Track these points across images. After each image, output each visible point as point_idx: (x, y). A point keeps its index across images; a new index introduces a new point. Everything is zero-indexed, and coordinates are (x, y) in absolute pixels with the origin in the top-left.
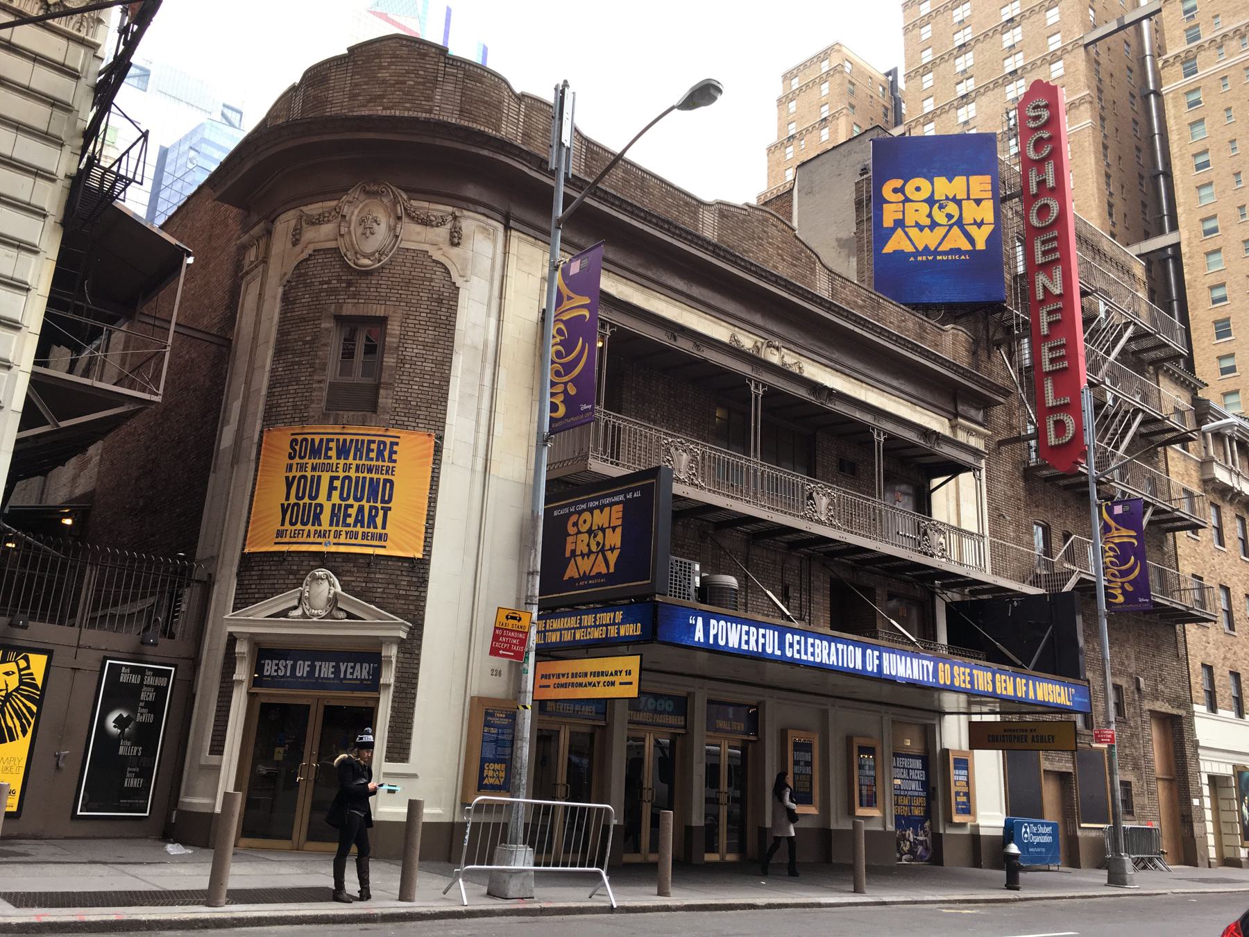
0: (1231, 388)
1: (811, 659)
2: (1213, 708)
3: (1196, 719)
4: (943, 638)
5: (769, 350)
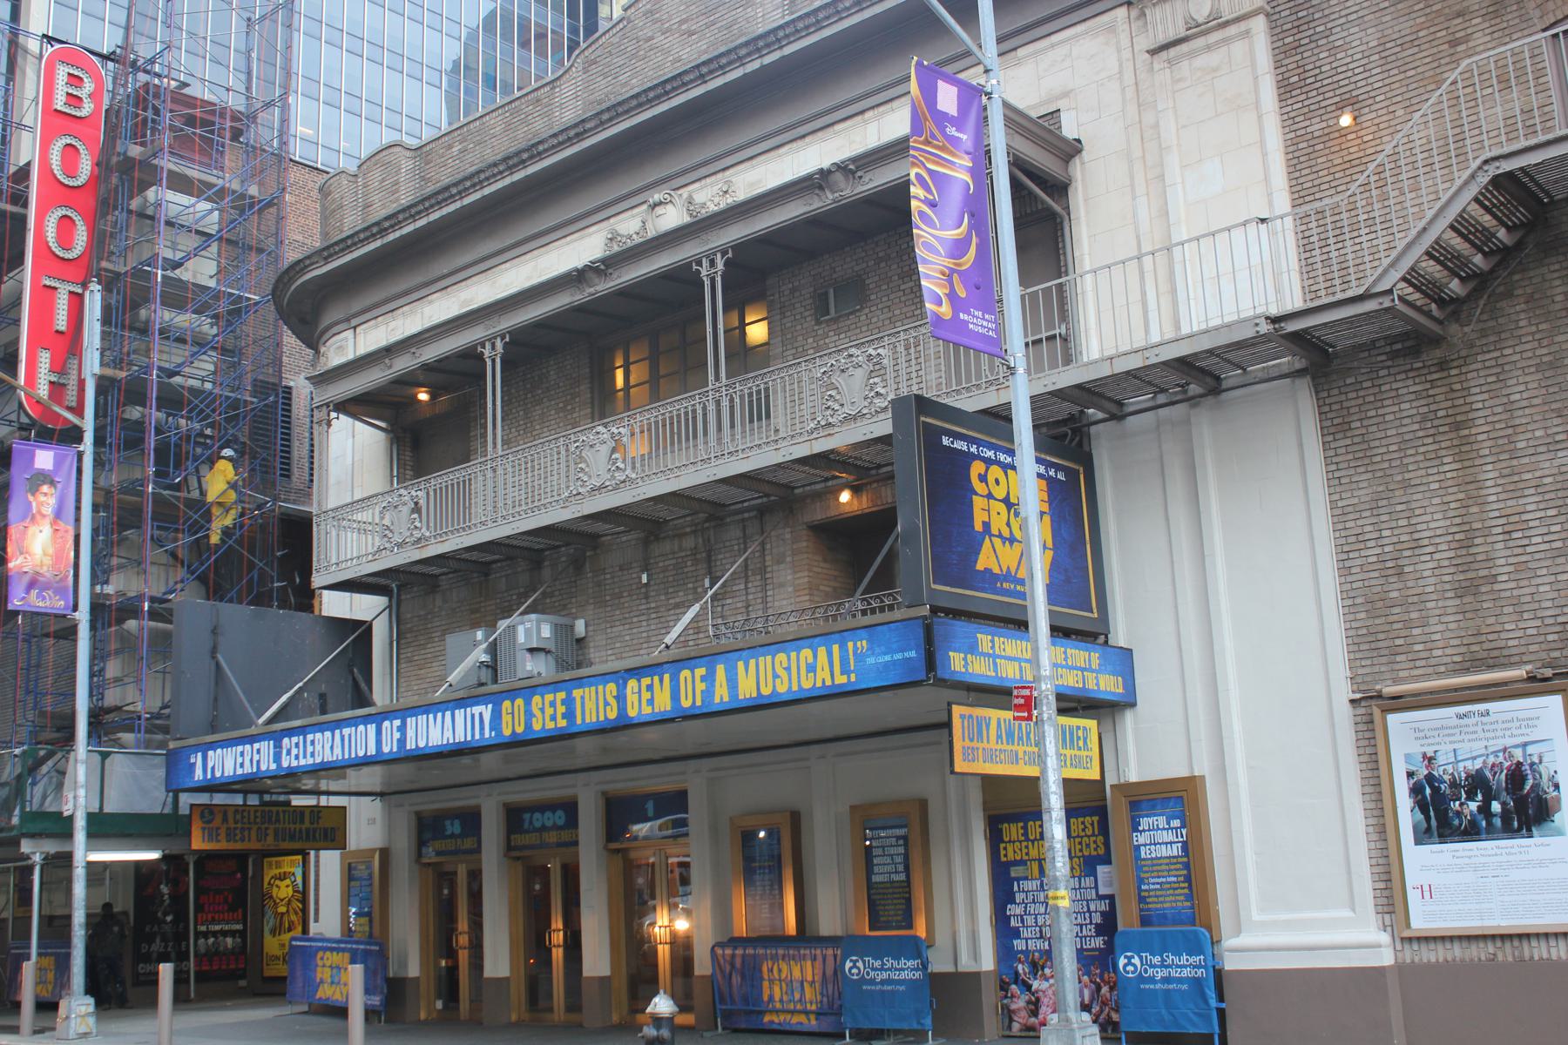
1: (310, 761)
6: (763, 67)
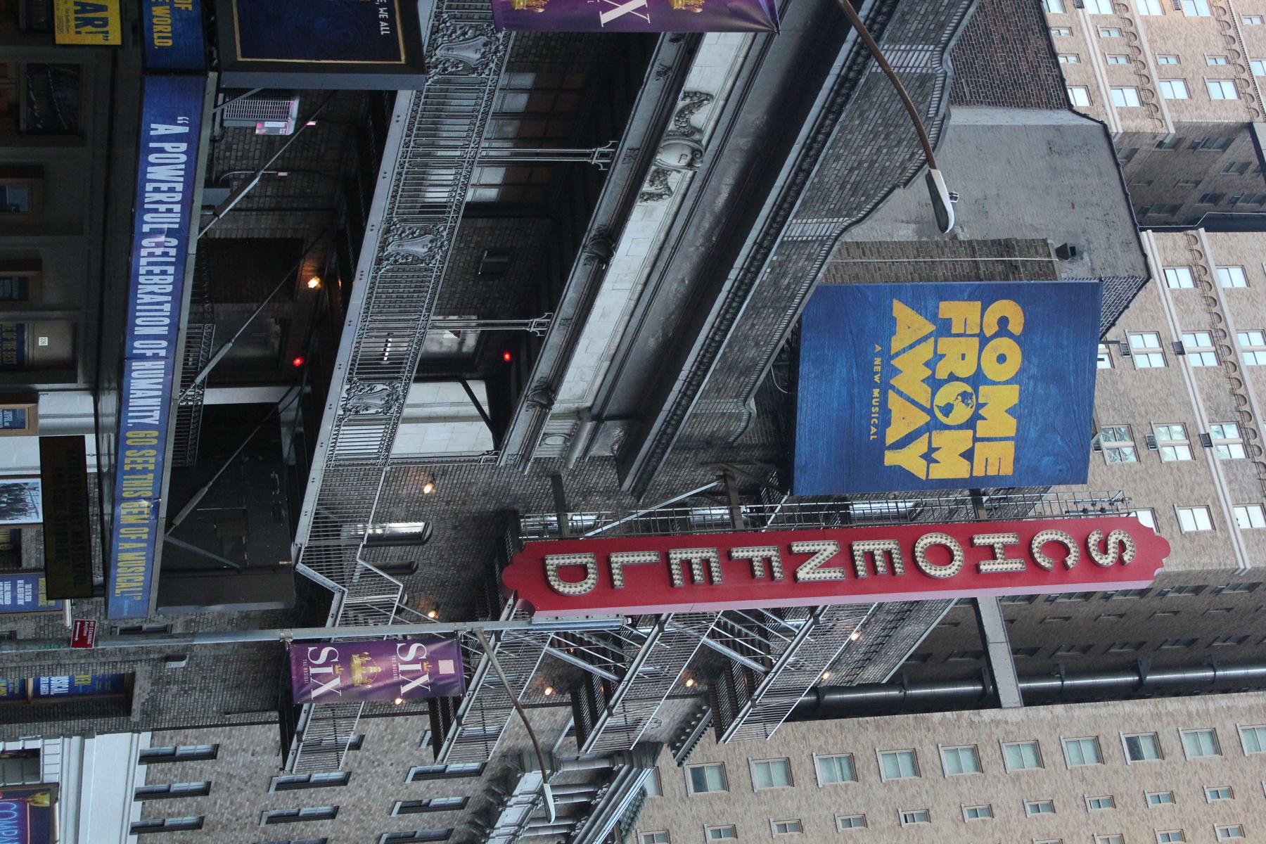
0: (732, 778)
1: (142, 271)
2: (146, 758)
3: (126, 736)
4: (214, 397)
5: (687, 152)
6: (726, 278)
